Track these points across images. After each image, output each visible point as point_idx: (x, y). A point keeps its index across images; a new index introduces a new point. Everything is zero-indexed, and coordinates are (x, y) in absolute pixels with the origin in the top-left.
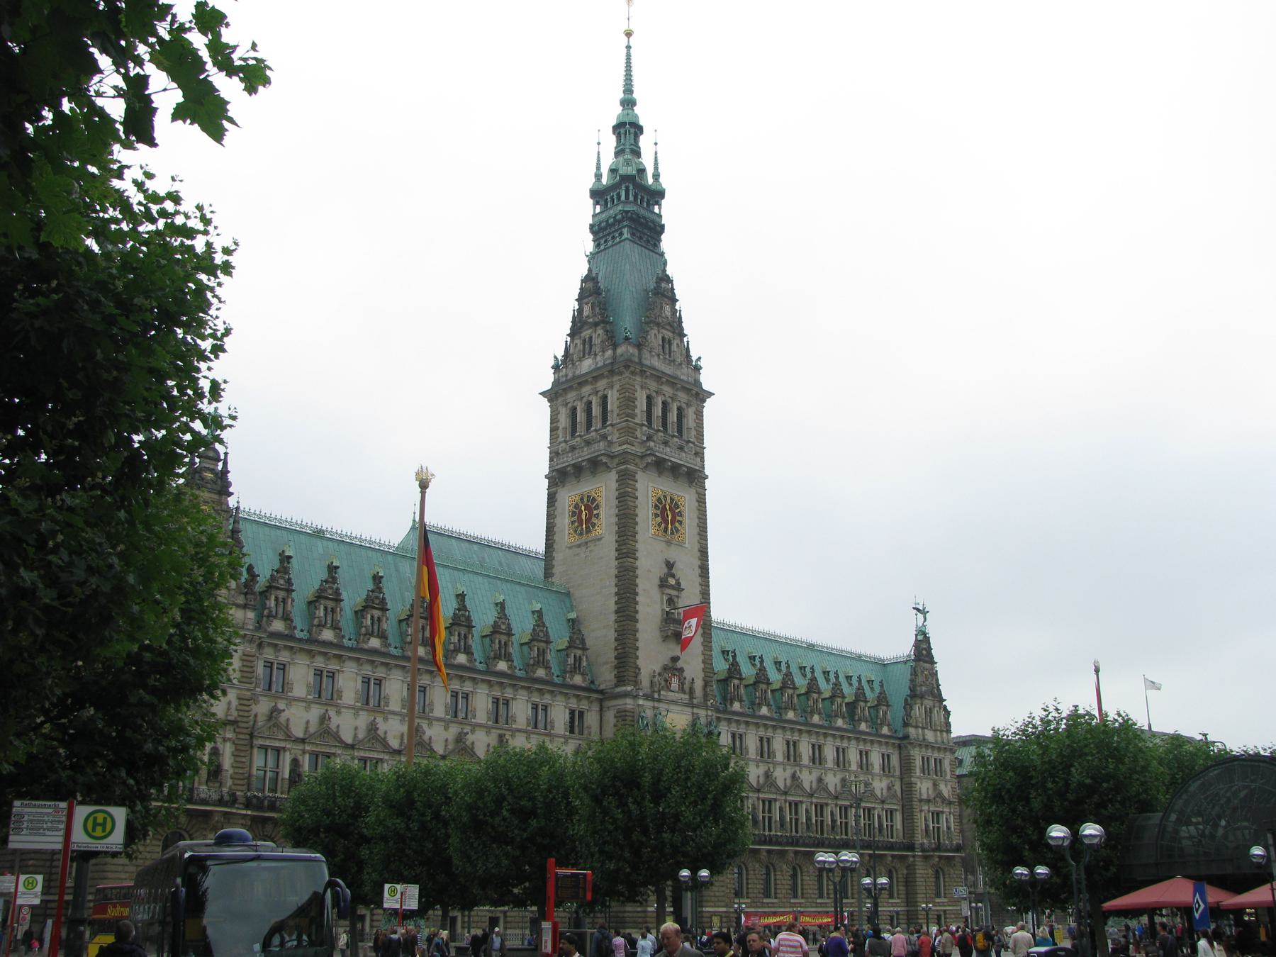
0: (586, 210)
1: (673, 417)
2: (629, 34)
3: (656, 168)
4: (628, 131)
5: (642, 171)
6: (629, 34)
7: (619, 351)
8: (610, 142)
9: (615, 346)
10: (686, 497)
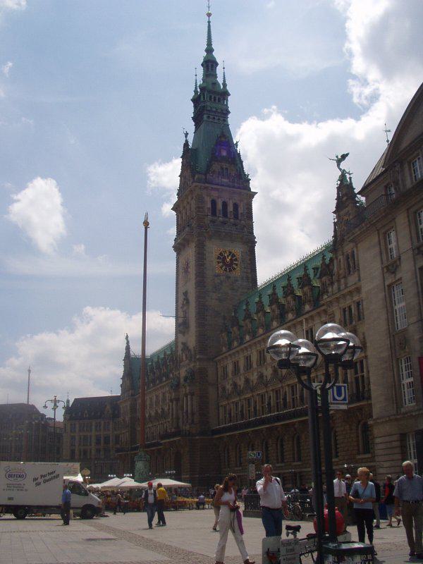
0: (190, 109)
1: (230, 208)
2: (209, 15)
3: (224, 81)
4: (210, 64)
5: (215, 84)
6: (209, 15)
7: (196, 176)
8: (201, 71)
9: (193, 177)
10: (238, 250)
